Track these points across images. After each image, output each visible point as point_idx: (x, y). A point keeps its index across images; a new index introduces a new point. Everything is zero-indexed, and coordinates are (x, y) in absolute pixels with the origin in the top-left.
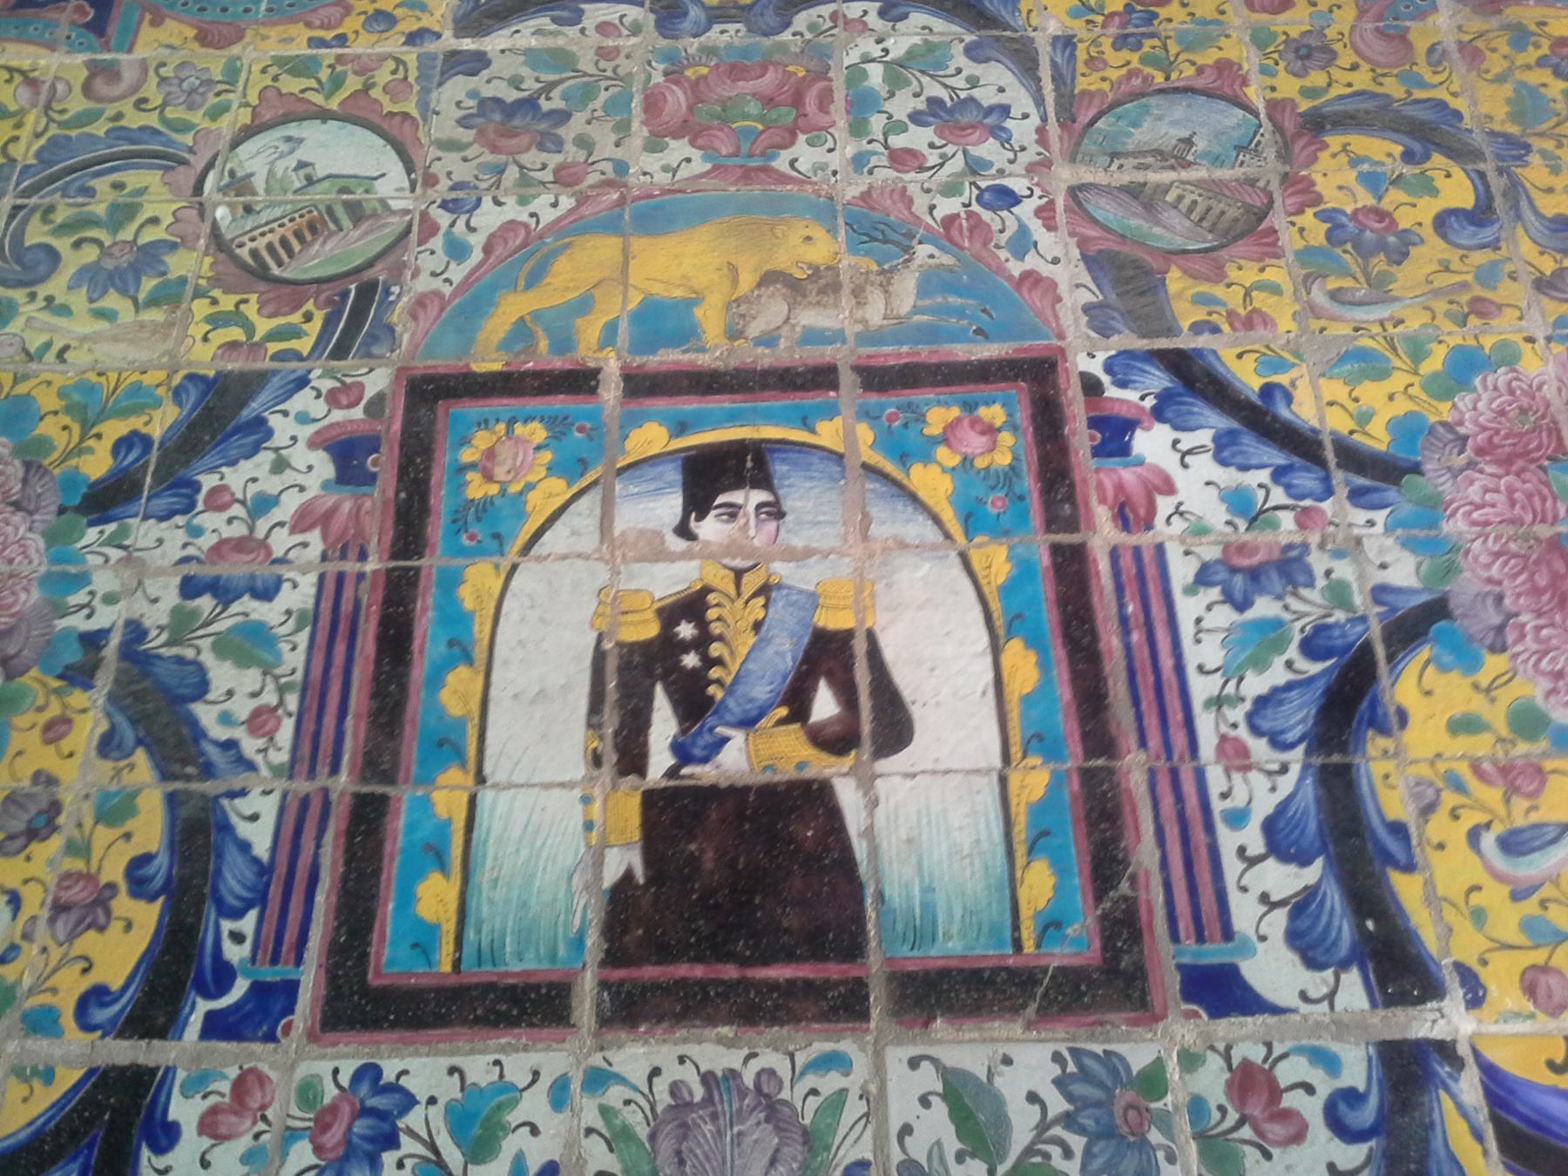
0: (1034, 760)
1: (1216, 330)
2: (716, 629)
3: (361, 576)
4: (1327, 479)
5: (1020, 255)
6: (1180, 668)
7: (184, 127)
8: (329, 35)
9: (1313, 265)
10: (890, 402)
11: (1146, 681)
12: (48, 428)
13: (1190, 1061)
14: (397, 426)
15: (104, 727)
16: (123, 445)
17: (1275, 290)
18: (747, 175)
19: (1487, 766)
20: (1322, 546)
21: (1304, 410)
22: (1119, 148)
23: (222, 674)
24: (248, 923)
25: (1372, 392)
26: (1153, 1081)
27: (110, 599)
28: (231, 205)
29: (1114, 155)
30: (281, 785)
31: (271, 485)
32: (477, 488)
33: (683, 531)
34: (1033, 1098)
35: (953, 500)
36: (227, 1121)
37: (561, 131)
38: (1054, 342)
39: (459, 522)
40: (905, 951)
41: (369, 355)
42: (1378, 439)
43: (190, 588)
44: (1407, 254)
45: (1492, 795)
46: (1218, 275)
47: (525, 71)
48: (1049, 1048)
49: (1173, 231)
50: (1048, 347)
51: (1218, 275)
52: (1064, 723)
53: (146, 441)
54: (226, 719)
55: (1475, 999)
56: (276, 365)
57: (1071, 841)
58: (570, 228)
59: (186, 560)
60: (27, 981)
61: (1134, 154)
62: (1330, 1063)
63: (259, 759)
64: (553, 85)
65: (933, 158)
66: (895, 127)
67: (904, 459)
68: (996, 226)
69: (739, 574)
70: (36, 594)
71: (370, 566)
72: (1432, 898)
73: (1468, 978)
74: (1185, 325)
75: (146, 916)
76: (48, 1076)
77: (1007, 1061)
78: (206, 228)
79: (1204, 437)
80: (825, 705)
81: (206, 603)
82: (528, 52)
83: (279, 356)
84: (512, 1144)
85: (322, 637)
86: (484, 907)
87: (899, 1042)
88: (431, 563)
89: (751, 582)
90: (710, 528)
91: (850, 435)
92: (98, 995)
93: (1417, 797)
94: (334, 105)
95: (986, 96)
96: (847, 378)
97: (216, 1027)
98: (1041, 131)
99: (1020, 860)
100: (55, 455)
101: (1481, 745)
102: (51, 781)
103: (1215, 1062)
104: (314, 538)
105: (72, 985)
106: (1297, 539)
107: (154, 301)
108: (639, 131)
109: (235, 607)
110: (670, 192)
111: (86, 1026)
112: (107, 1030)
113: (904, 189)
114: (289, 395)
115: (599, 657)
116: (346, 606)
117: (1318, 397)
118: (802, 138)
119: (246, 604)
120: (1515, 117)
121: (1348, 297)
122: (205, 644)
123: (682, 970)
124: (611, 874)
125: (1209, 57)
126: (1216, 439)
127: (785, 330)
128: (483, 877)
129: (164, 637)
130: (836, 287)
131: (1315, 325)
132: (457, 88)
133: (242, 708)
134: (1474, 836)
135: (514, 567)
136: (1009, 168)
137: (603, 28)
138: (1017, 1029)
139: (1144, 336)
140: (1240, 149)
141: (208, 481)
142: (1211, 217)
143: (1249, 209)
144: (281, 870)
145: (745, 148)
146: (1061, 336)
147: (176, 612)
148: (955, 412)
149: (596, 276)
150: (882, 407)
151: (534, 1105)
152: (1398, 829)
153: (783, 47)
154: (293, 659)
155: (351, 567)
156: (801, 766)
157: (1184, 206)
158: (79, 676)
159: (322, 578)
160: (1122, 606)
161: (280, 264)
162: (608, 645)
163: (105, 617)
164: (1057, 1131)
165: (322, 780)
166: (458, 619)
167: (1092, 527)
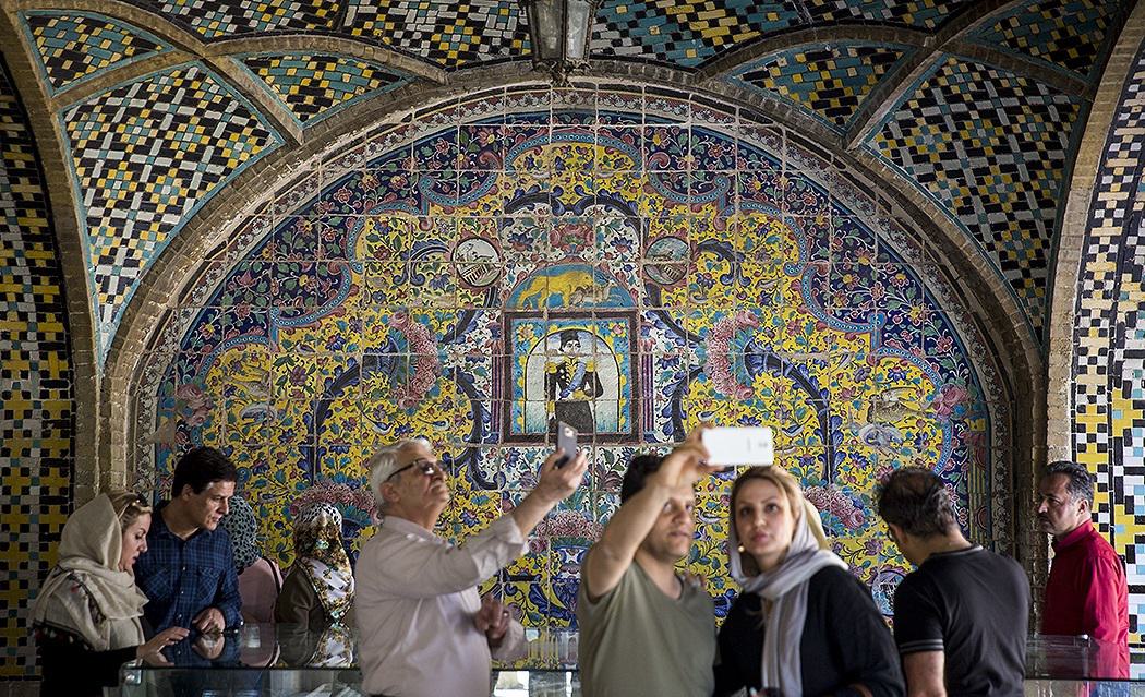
7: (445, 240)
10: (602, 321)
16: (451, 326)
17: (683, 295)
21: (683, 326)
23: (477, 377)
25: (698, 321)
32: (521, 339)
33: (561, 350)
49: (664, 278)
57: (628, 413)
80: (587, 387)
90: (566, 349)
91: (594, 330)
105: (461, 434)
107: (448, 291)
120: (744, 248)
132: (506, 230)
141: (467, 336)
151: (539, 454)
152: (685, 412)
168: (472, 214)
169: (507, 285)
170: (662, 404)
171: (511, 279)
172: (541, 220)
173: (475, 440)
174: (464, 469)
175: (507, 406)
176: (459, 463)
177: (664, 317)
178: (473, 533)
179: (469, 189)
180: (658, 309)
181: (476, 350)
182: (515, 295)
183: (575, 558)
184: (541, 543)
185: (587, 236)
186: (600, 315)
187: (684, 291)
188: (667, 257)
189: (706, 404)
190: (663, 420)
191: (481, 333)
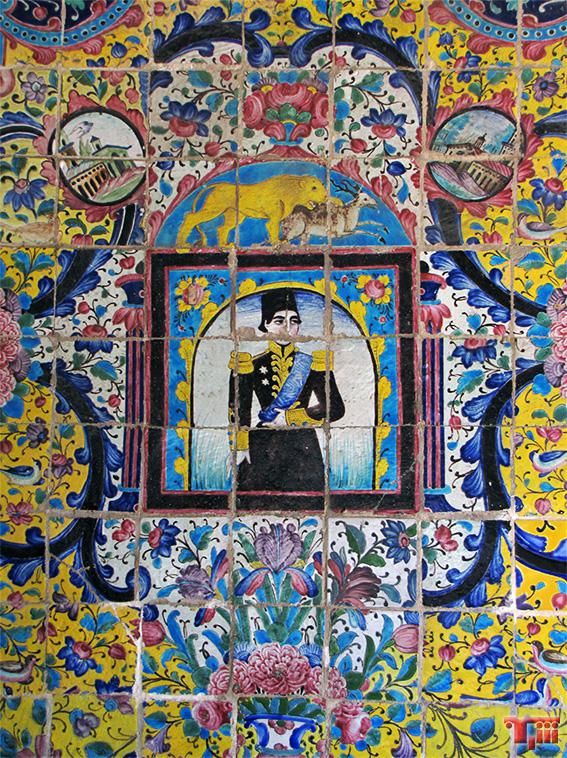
0: (386, 423)
1: (477, 242)
2: (275, 369)
3: (142, 343)
4: (509, 314)
5: (402, 201)
6: (441, 390)
7: (37, 113)
8: (96, 59)
9: (525, 209)
10: (344, 272)
11: (429, 394)
12: (11, 274)
13: (424, 525)
14: (149, 278)
15: (57, 401)
16: (43, 282)
17: (506, 222)
18: (290, 151)
19: (542, 430)
20: (501, 342)
21: (505, 283)
22: (452, 142)
23: (96, 382)
24: (119, 473)
25: (534, 274)
26: (412, 530)
27: (49, 350)
28: (66, 160)
29: (449, 146)
30: (123, 425)
31: (103, 302)
32: (183, 308)
33: (262, 328)
34: (374, 535)
35: (366, 318)
36: (121, 536)
37: (207, 124)
38: (412, 246)
39: (176, 319)
40: (337, 488)
41: (135, 243)
42: (532, 296)
43: (79, 346)
44: (563, 205)
45: (541, 441)
46: (482, 214)
47: (189, 86)
48: (380, 520)
49: (468, 190)
50: (409, 248)
51: (482, 214)
52: (398, 411)
53: (51, 280)
54: (100, 399)
55: (520, 507)
56: (98, 246)
57: (394, 452)
58: (213, 179)
59: (75, 334)
60: (49, 491)
61: (458, 146)
62: (469, 527)
63: (114, 415)
64: (202, 95)
65: (370, 146)
66: (355, 126)
67: (348, 300)
68: (394, 185)
69: (283, 347)
70: (21, 347)
71: (145, 340)
72: (513, 476)
73: (518, 501)
74: (465, 240)
75: (85, 469)
76: (61, 520)
77: (367, 523)
78: (57, 174)
79: (465, 293)
80: (314, 401)
81: (85, 353)
82: (190, 73)
83: (99, 242)
84: (211, 545)
85: (130, 369)
86: (196, 470)
87: (332, 517)
88: (167, 339)
89: (288, 350)
90: (272, 327)
92: (72, 496)
93: (515, 440)
94: (103, 103)
95: (397, 109)
96: (327, 260)
97: (113, 507)
98: (419, 131)
99: (377, 459)
100: (16, 286)
101: (542, 422)
102: (43, 422)
103: (432, 525)
104: (122, 325)
105: (63, 493)
106: (493, 338)
107: (42, 212)
108: (242, 125)
109: (97, 355)
110: (255, 161)
111: (71, 506)
112: (79, 506)
113: (357, 162)
114: (105, 261)
115: (232, 379)
116: (138, 356)
117: (512, 276)
118: (313, 131)
119: (100, 353)
121: (534, 227)
122: (88, 369)
123: (264, 492)
124: (239, 460)
125: (499, 88)
126: (469, 294)
127: (303, 237)
128: (196, 457)
129: (72, 366)
130: (325, 215)
131: (518, 240)
132: (159, 95)
133: (106, 396)
134: (531, 455)
135: (199, 341)
136: (403, 152)
137: (224, 58)
138: (371, 514)
139: (448, 244)
140: (504, 143)
141: (78, 300)
142: (485, 183)
143: (502, 178)
144: (128, 455)
145: (288, 135)
146: (415, 244)
147: (75, 356)
148: (370, 278)
149: (225, 206)
150: (341, 275)
151: (218, 533)
152: (507, 451)
153: (306, 73)
154: (122, 377)
155: (138, 339)
156: (304, 423)
157: (474, 176)
158: (44, 380)
159: (127, 343)
160: (424, 364)
161: (92, 194)
162: (235, 375)
163: (49, 358)
164: (380, 545)
165: (138, 423)
166: (179, 362)
167: (417, 331)
168: (90, 63)
169: (157, 201)
170: (461, 437)
171: (166, 190)
172: (225, 75)
173: (92, 498)
174: (70, 560)
175: (155, 438)
176: (59, 547)
177: (466, 265)
178: (83, 688)
179: (85, 14)
180: (455, 248)
181: (96, 328)
182: (173, 220)
183: (285, 739)
184: (218, 707)
185: (314, 108)
186: (340, 261)
187: (507, 214)
188: (475, 148)
189: (551, 435)
190: (464, 467)
191: (106, 296)
